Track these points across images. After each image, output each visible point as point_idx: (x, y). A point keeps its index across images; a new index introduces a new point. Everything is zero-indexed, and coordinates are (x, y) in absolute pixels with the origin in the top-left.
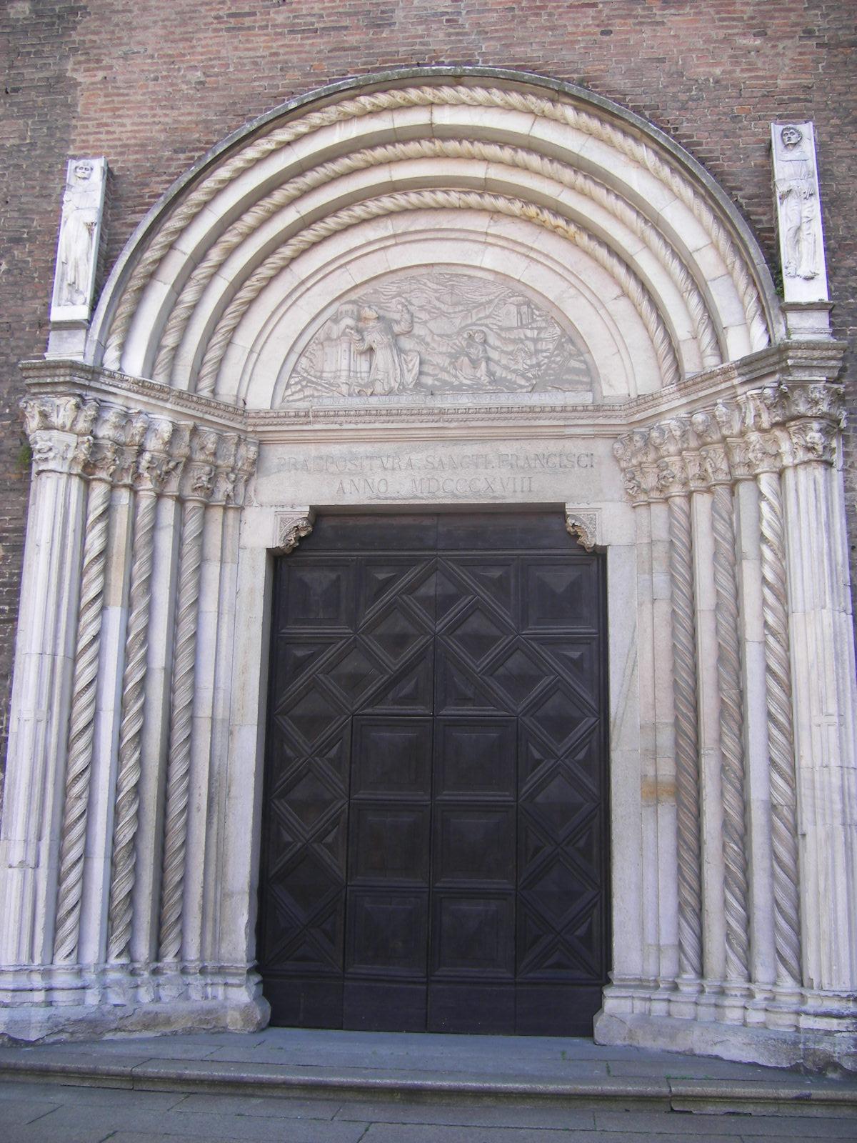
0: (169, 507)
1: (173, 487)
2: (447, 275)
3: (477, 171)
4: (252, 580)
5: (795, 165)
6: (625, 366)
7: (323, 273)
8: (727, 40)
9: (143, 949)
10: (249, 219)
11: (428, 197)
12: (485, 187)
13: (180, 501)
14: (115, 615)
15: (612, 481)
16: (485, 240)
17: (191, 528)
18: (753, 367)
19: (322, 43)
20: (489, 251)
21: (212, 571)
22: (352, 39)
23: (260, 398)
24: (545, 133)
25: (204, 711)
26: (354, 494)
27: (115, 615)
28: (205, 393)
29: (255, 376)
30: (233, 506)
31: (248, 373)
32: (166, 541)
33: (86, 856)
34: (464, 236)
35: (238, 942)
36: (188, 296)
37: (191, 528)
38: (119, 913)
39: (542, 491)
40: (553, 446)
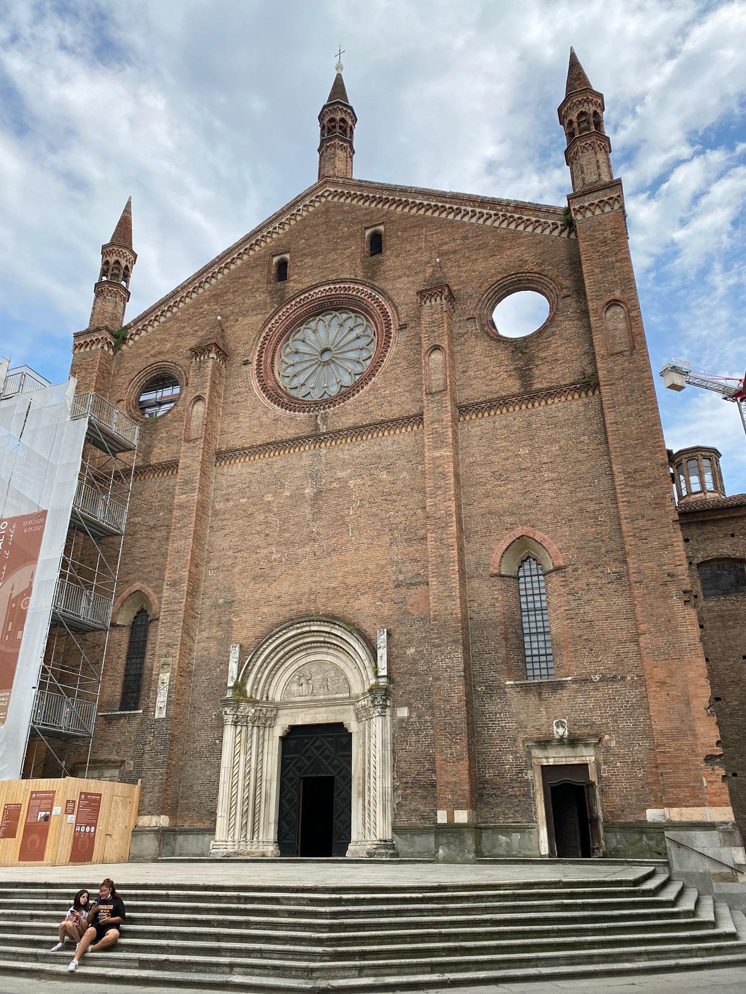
0: (255, 728)
1: (256, 724)
3: (322, 639)
5: (382, 640)
7: (292, 664)
8: (374, 603)
9: (249, 837)
10: (272, 655)
11: (313, 645)
12: (325, 642)
13: (258, 727)
14: (242, 756)
15: (354, 718)
16: (327, 653)
17: (261, 733)
19: (288, 608)
20: (329, 657)
21: (266, 743)
22: (293, 607)
23: (278, 699)
24: (333, 631)
25: (264, 778)
26: (299, 722)
27: (242, 756)
28: (264, 699)
31: (275, 692)
32: (255, 737)
33: (235, 814)
34: (323, 653)
36: (259, 676)
37: (261, 733)
38: (244, 826)
40: (341, 707)
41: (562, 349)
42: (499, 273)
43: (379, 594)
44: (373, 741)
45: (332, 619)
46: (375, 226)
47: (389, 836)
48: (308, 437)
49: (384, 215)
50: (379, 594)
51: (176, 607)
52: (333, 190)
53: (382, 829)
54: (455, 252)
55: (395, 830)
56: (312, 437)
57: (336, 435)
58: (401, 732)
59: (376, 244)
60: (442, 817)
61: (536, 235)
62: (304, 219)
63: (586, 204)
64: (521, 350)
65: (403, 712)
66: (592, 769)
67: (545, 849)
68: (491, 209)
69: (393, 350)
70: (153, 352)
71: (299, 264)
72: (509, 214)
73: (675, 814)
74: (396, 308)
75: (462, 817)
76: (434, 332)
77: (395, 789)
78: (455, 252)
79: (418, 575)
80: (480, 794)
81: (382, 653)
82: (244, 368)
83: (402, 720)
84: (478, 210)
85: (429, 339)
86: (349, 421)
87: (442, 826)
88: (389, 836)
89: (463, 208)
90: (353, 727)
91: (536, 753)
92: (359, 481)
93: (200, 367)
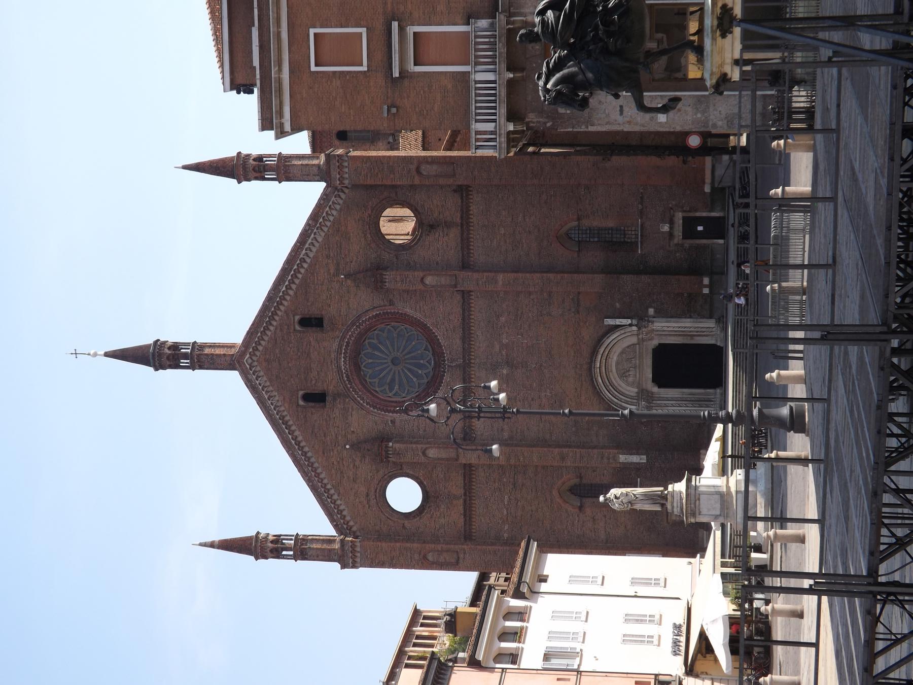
2: (617, 364)
4: (662, 390)
5: (610, 322)
6: (634, 340)
18: (639, 329)
29: (633, 391)
30: (652, 393)
35: (711, 391)
39: (651, 351)
41: (435, 201)
43: (582, 324)
44: (665, 329)
45: (594, 353)
47: (714, 321)
48: (464, 373)
49: (287, 315)
50: (582, 324)
51: (578, 455)
52: (248, 356)
53: (711, 324)
54: (338, 264)
55: (711, 317)
56: (464, 369)
57: (467, 351)
58: (662, 313)
59: (312, 322)
60: (706, 291)
62: (270, 380)
64: (425, 226)
65: (651, 311)
66: (686, 215)
67: (721, 241)
69: (408, 311)
70: (365, 502)
71: (314, 382)
73: (708, 179)
74: (375, 308)
75: (706, 281)
77: (691, 317)
78: (338, 264)
79: (573, 299)
80: (695, 271)
81: (618, 322)
82: (398, 423)
83: (655, 312)
84: (307, 246)
86: (458, 342)
87: (710, 291)
88: (714, 321)
89: (301, 256)
90: (655, 342)
91: (676, 241)
92: (504, 336)
93: (399, 454)
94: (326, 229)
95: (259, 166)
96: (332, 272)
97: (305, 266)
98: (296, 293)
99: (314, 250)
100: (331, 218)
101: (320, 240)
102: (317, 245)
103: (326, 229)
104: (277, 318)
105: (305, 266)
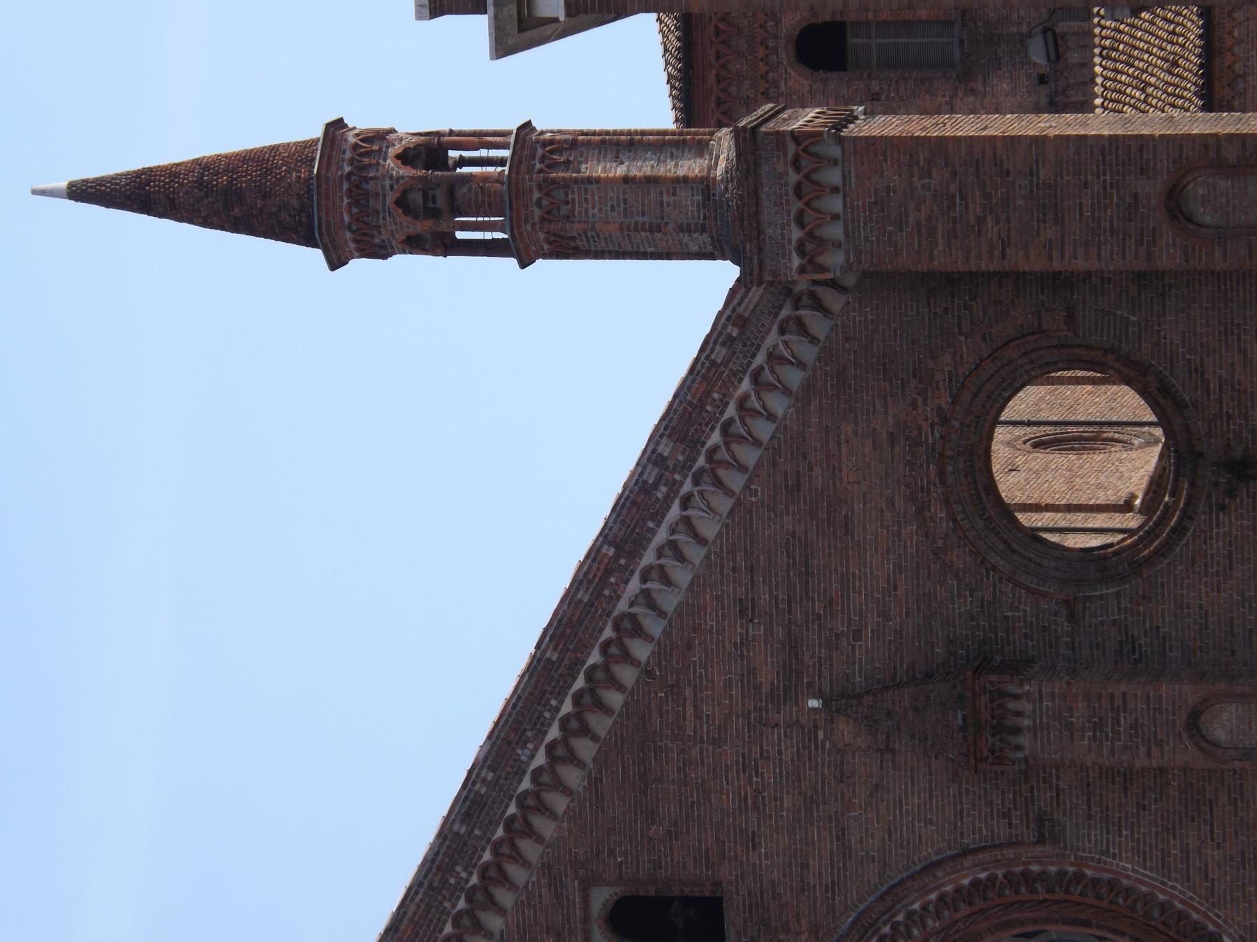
42: (920, 512)
46: (586, 919)
61: (808, 386)
63: (796, 234)
68: (658, 517)
72: (701, 461)
74: (966, 852)
76: (1135, 726)
84: (649, 558)
85: (1160, 744)
89: (622, 606)
94: (736, 481)
95: (427, 187)
96: (766, 677)
97: (641, 650)
98: (595, 782)
99: (683, 576)
100: (764, 430)
101: (709, 529)
102: (695, 553)
103: (736, 481)
104: (505, 897)
105: (641, 650)
